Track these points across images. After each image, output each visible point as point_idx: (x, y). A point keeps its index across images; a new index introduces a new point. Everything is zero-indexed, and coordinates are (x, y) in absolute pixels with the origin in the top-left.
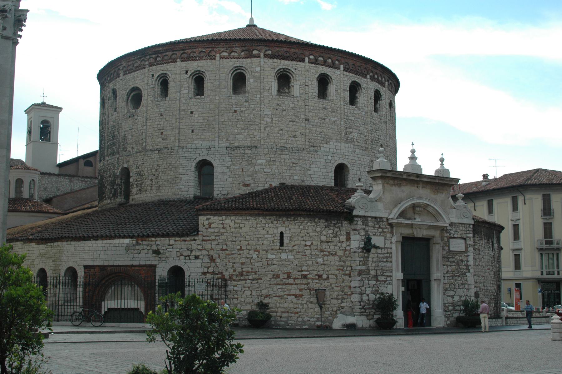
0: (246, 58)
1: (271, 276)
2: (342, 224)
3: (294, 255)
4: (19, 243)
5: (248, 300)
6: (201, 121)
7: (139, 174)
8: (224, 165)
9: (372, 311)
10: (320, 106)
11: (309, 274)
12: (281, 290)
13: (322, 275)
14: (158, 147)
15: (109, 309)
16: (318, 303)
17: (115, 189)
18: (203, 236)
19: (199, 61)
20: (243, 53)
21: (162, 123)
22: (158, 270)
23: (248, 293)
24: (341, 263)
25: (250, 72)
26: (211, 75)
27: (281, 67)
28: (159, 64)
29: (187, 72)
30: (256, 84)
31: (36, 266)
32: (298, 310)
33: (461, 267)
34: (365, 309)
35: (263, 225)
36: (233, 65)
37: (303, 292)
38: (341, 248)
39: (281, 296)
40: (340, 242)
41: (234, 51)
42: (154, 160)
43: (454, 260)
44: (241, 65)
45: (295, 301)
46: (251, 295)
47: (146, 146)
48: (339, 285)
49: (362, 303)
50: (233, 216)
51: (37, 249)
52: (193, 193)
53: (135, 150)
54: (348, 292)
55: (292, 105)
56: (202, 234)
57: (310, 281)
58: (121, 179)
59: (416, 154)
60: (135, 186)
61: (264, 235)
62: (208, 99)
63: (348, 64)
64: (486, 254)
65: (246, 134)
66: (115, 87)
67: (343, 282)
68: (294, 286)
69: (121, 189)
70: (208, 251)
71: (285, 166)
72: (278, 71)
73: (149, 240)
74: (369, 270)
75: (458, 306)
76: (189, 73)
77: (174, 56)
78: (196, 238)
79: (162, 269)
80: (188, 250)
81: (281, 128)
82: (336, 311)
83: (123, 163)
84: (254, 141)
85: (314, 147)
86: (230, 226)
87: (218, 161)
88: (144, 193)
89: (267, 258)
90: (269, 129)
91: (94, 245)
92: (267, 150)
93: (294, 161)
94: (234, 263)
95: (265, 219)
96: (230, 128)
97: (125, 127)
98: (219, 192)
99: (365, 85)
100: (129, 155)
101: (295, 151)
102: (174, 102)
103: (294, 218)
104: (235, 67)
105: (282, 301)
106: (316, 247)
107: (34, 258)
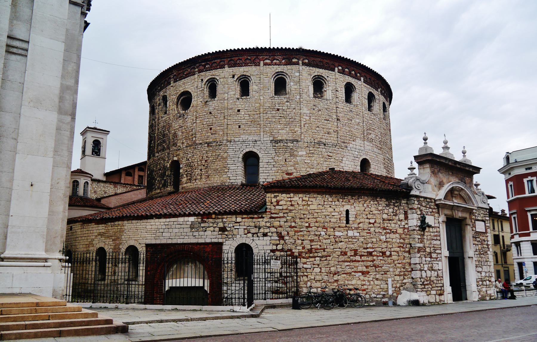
0: (286, 65)
1: (340, 253)
3: (359, 232)
4: (78, 224)
5: (318, 278)
6: (248, 118)
7: (189, 165)
8: (269, 156)
9: (429, 287)
10: (348, 109)
11: (374, 252)
12: (348, 267)
13: (385, 252)
14: (207, 141)
17: (165, 180)
18: (272, 214)
19: (245, 67)
20: (283, 61)
21: (211, 120)
22: (225, 247)
23: (317, 270)
24: (402, 241)
25: (290, 76)
29: (233, 77)
30: (296, 87)
31: (95, 245)
32: (365, 287)
34: (424, 285)
35: (330, 203)
37: (370, 269)
38: (401, 226)
39: (349, 273)
42: (204, 152)
45: (362, 278)
46: (320, 272)
48: (401, 262)
49: (422, 279)
50: (301, 193)
51: (97, 228)
52: (240, 181)
54: (408, 269)
55: (326, 107)
56: (270, 212)
57: (375, 258)
58: (171, 171)
59: (448, 145)
60: (185, 176)
61: (331, 212)
63: (366, 77)
65: (288, 129)
66: (166, 94)
67: (404, 259)
68: (360, 263)
70: (276, 228)
71: (322, 157)
72: (314, 77)
74: (425, 247)
76: (236, 77)
78: (263, 216)
79: (228, 247)
80: (256, 227)
82: (399, 288)
83: (174, 157)
84: (295, 136)
85: (344, 143)
86: (298, 204)
88: (194, 181)
89: (334, 236)
90: (307, 125)
91: (157, 223)
92: (307, 143)
94: (303, 240)
95: (331, 197)
96: (274, 124)
97: (176, 125)
98: (264, 180)
99: (377, 96)
100: (179, 150)
101: (330, 146)
103: (359, 196)
104: (277, 73)
105: (350, 279)
106: (379, 225)
107: (94, 237)
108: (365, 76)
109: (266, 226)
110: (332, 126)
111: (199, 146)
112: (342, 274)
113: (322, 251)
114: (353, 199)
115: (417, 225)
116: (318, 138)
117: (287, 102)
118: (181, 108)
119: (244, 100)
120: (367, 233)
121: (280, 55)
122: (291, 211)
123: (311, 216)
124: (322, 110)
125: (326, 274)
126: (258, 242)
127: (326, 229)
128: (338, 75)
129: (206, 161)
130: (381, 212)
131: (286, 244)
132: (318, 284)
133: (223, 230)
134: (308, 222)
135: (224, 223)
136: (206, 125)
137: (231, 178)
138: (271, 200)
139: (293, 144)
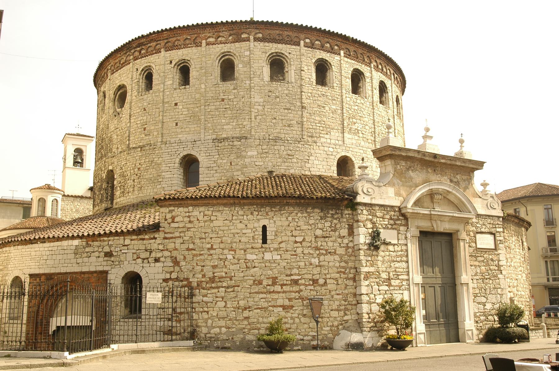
0: (234, 42)
1: (252, 282)
2: (342, 214)
5: (222, 314)
7: (123, 175)
8: (210, 160)
11: (300, 279)
12: (264, 300)
13: (318, 280)
14: (141, 144)
15: (58, 328)
16: (313, 317)
17: (102, 194)
19: (184, 50)
20: (230, 38)
21: (145, 118)
22: (110, 277)
24: (343, 264)
26: (196, 63)
27: (273, 51)
28: (143, 57)
30: (245, 69)
33: (491, 267)
36: (220, 50)
38: (342, 245)
40: (340, 237)
41: (222, 36)
43: (483, 259)
44: (228, 50)
45: (283, 313)
46: (225, 307)
47: (129, 144)
48: (340, 292)
49: (370, 315)
50: (202, 206)
53: (120, 150)
54: (352, 301)
55: (286, 92)
56: (163, 231)
57: (302, 287)
60: (118, 188)
61: (241, 229)
62: (194, 88)
63: (349, 50)
64: (517, 253)
65: (234, 124)
66: (105, 89)
68: (281, 294)
69: (107, 194)
70: (171, 252)
71: (279, 158)
72: (270, 55)
73: (100, 241)
75: (491, 315)
77: (158, 47)
78: (156, 236)
79: (115, 275)
80: (146, 250)
81: (274, 116)
82: (337, 327)
84: (243, 132)
85: (312, 137)
86: (198, 220)
87: (204, 155)
89: (245, 259)
90: (260, 117)
91: (41, 249)
93: (289, 152)
94: (204, 266)
95: (242, 209)
100: (113, 157)
102: (158, 94)
103: (281, 207)
104: (223, 53)
108: (347, 48)
109: (158, 249)
110: (294, 117)
111: (132, 151)
112: (255, 309)
113: (229, 279)
114: (272, 211)
115: (365, 242)
116: (274, 132)
117: (234, 89)
118: (119, 105)
119: (182, 91)
120: (292, 255)
121: (226, 31)
122: (189, 229)
123: (214, 235)
124: (280, 97)
125: (233, 309)
126: (148, 270)
127: (235, 251)
128: (304, 50)
129: (139, 169)
130: (313, 226)
131: (182, 271)
132: (222, 323)
133: (109, 254)
134: (210, 243)
135: (110, 246)
136: (140, 124)
137: (166, 189)
138: (166, 216)
139: (240, 142)
